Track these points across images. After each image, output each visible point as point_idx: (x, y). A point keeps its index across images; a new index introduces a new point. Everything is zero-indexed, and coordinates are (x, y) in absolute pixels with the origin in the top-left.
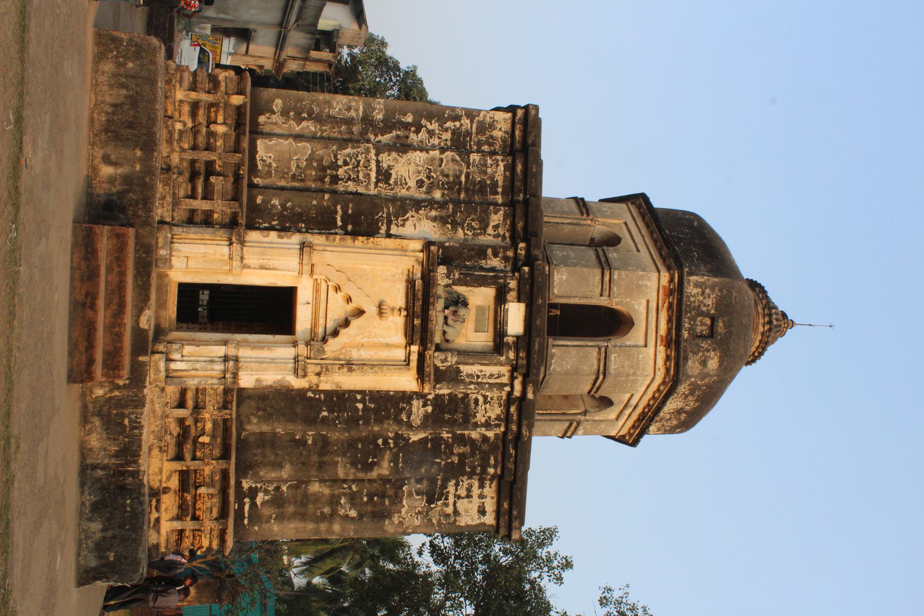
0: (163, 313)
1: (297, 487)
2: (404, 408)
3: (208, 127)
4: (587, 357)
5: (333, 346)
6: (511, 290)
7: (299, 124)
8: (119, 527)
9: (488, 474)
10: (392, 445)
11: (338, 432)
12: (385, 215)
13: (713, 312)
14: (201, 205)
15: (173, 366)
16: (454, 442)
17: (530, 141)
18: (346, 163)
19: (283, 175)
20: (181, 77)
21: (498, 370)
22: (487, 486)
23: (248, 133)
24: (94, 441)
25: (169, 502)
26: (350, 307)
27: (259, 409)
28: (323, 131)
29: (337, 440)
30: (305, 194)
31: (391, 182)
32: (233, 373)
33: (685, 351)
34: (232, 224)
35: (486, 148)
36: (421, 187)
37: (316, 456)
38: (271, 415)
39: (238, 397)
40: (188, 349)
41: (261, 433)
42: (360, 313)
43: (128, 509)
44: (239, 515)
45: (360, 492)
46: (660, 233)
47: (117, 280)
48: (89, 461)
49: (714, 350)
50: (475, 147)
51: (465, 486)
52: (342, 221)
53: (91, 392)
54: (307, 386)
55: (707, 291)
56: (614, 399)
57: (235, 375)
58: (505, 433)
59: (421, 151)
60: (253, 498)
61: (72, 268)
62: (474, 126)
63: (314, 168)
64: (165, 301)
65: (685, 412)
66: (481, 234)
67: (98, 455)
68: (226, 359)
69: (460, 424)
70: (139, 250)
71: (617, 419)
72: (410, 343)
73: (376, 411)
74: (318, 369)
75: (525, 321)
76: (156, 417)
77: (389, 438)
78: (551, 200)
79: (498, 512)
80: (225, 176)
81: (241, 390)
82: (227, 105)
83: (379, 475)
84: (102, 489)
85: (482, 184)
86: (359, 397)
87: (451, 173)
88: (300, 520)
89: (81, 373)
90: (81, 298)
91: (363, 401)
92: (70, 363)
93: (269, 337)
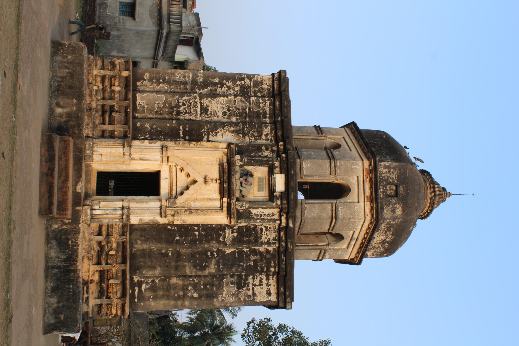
0: (89, 186)
1: (164, 280)
2: (221, 234)
3: (110, 88)
5: (180, 200)
7: (158, 85)
8: (66, 301)
9: (271, 272)
10: (216, 256)
11: (186, 248)
12: (206, 131)
13: (396, 182)
14: (108, 127)
15: (95, 212)
16: (250, 254)
17: (282, 89)
18: (184, 104)
19: (151, 111)
20: (96, 63)
21: (273, 212)
22: (271, 278)
23: (131, 91)
24: (53, 254)
25: (93, 288)
27: (141, 236)
28: (171, 89)
29: (185, 253)
31: (209, 113)
32: (127, 216)
33: (382, 205)
34: (124, 137)
35: (259, 94)
36: (225, 115)
38: (148, 239)
39: (130, 230)
40: (102, 204)
41: (143, 250)
42: (195, 182)
43: (71, 290)
44: (132, 296)
45: (199, 283)
46: (363, 141)
47: (64, 163)
48: (50, 264)
50: (253, 94)
51: (258, 279)
52: (183, 134)
53: (51, 227)
55: (392, 170)
56: (344, 235)
57: (128, 217)
58: (279, 248)
59: (224, 96)
60: (140, 287)
61: (41, 155)
62: (252, 83)
63: (167, 108)
65: (387, 242)
66: (258, 139)
68: (123, 208)
69: (253, 243)
70: (76, 151)
71: (347, 248)
72: (222, 198)
73: (206, 236)
74: (173, 213)
75: (285, 184)
76: (85, 241)
77: (214, 251)
78: (300, 128)
79: (278, 294)
80: (119, 112)
81: (132, 225)
82: (120, 76)
83: (209, 272)
84: (57, 279)
85: (258, 113)
86: (196, 228)
87: (240, 108)
88: (166, 299)
89: (46, 211)
90: (45, 170)
91: (198, 230)
92: (40, 205)
93: (146, 197)
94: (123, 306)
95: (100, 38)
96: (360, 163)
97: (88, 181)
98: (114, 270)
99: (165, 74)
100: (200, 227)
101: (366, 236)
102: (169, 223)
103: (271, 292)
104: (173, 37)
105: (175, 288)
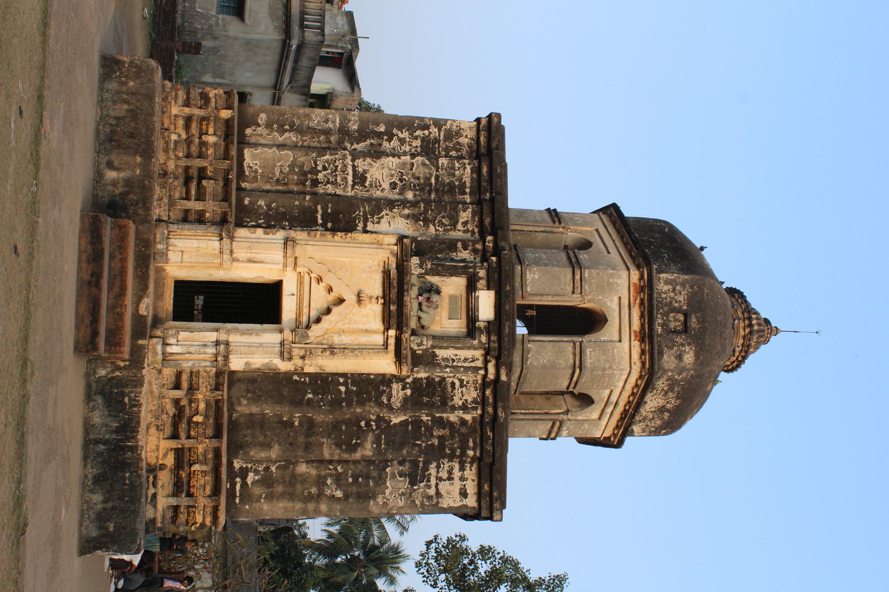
0: (160, 304)
2: (384, 391)
3: (200, 138)
4: (562, 351)
5: (315, 331)
6: (481, 278)
7: (282, 135)
8: (119, 499)
9: (468, 456)
10: (374, 428)
13: (685, 308)
14: (194, 205)
15: (169, 349)
17: (494, 145)
18: (325, 168)
21: (473, 354)
22: (468, 468)
23: (235, 143)
24: (97, 418)
25: (165, 478)
26: (332, 297)
27: (248, 391)
28: (303, 141)
29: (322, 422)
30: (288, 195)
31: (367, 184)
33: (660, 346)
34: (223, 222)
35: (453, 153)
36: (394, 188)
37: (302, 437)
38: (259, 397)
39: (229, 380)
40: (183, 335)
41: (251, 415)
42: (341, 301)
43: (127, 482)
44: (231, 494)
45: (345, 473)
46: (629, 235)
47: (119, 265)
48: (92, 437)
49: (689, 344)
51: (446, 468)
52: (322, 219)
53: (95, 373)
54: (293, 369)
55: (678, 288)
56: (594, 397)
57: (226, 358)
58: (482, 416)
59: (394, 157)
61: (80, 251)
62: (442, 134)
63: (296, 173)
64: (163, 293)
65: (667, 410)
66: (451, 230)
67: (100, 431)
68: (217, 343)
69: (438, 407)
71: (600, 419)
72: (387, 329)
73: (358, 394)
74: (302, 353)
75: (495, 307)
76: (153, 398)
77: (371, 420)
78: (522, 213)
79: (479, 495)
81: (232, 373)
82: (217, 119)
83: (363, 456)
84: (103, 462)
85: (451, 186)
86: (341, 380)
87: (421, 176)
88: (289, 500)
89: (86, 346)
90: (86, 277)
91: (345, 384)
92: (77, 335)
93: (258, 326)
94: (215, 510)
95: (184, 52)
96: (624, 274)
97: (159, 296)
98: (201, 448)
99: (294, 115)
100: (348, 378)
101: (631, 398)
102: (296, 370)
103: (468, 491)
104: (308, 53)
105: (304, 482)
